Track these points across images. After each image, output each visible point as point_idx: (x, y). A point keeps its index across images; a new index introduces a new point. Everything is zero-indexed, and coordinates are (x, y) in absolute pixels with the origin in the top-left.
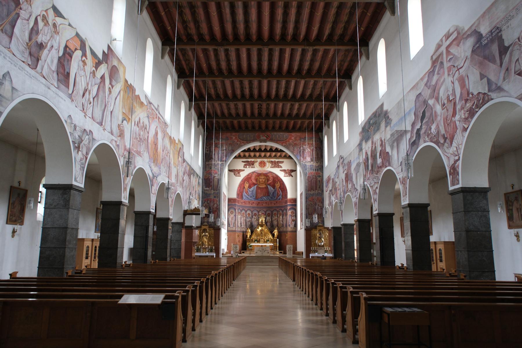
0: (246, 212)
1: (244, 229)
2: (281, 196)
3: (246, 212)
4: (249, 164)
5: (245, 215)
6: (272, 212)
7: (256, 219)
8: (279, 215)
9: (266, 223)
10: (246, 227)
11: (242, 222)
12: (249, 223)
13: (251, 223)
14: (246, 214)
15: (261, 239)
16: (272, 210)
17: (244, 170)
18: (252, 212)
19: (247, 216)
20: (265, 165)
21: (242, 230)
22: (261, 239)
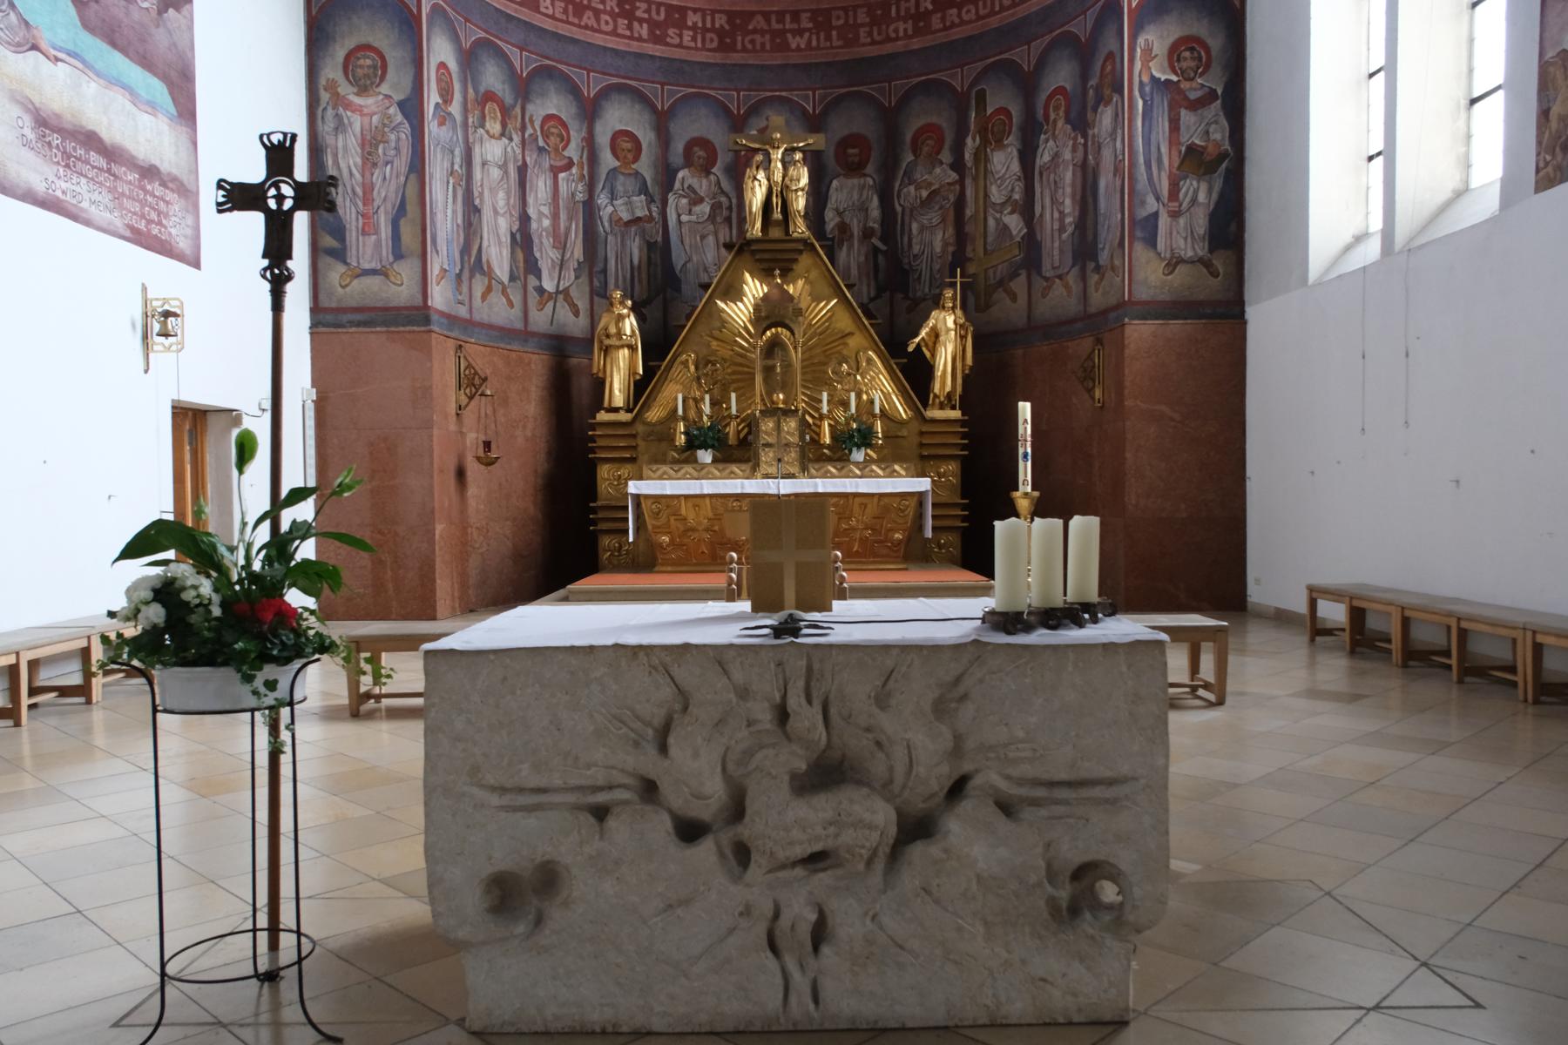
0: (590, 111)
1: (564, 313)
3: (590, 111)
5: (573, 151)
6: (891, 120)
7: (705, 208)
8: (971, 143)
9: (827, 239)
10: (600, 294)
11: (541, 223)
12: (636, 249)
13: (659, 251)
14: (590, 143)
15: (768, 425)
18: (662, 122)
19: (608, 160)
21: (540, 320)
22: (768, 425)
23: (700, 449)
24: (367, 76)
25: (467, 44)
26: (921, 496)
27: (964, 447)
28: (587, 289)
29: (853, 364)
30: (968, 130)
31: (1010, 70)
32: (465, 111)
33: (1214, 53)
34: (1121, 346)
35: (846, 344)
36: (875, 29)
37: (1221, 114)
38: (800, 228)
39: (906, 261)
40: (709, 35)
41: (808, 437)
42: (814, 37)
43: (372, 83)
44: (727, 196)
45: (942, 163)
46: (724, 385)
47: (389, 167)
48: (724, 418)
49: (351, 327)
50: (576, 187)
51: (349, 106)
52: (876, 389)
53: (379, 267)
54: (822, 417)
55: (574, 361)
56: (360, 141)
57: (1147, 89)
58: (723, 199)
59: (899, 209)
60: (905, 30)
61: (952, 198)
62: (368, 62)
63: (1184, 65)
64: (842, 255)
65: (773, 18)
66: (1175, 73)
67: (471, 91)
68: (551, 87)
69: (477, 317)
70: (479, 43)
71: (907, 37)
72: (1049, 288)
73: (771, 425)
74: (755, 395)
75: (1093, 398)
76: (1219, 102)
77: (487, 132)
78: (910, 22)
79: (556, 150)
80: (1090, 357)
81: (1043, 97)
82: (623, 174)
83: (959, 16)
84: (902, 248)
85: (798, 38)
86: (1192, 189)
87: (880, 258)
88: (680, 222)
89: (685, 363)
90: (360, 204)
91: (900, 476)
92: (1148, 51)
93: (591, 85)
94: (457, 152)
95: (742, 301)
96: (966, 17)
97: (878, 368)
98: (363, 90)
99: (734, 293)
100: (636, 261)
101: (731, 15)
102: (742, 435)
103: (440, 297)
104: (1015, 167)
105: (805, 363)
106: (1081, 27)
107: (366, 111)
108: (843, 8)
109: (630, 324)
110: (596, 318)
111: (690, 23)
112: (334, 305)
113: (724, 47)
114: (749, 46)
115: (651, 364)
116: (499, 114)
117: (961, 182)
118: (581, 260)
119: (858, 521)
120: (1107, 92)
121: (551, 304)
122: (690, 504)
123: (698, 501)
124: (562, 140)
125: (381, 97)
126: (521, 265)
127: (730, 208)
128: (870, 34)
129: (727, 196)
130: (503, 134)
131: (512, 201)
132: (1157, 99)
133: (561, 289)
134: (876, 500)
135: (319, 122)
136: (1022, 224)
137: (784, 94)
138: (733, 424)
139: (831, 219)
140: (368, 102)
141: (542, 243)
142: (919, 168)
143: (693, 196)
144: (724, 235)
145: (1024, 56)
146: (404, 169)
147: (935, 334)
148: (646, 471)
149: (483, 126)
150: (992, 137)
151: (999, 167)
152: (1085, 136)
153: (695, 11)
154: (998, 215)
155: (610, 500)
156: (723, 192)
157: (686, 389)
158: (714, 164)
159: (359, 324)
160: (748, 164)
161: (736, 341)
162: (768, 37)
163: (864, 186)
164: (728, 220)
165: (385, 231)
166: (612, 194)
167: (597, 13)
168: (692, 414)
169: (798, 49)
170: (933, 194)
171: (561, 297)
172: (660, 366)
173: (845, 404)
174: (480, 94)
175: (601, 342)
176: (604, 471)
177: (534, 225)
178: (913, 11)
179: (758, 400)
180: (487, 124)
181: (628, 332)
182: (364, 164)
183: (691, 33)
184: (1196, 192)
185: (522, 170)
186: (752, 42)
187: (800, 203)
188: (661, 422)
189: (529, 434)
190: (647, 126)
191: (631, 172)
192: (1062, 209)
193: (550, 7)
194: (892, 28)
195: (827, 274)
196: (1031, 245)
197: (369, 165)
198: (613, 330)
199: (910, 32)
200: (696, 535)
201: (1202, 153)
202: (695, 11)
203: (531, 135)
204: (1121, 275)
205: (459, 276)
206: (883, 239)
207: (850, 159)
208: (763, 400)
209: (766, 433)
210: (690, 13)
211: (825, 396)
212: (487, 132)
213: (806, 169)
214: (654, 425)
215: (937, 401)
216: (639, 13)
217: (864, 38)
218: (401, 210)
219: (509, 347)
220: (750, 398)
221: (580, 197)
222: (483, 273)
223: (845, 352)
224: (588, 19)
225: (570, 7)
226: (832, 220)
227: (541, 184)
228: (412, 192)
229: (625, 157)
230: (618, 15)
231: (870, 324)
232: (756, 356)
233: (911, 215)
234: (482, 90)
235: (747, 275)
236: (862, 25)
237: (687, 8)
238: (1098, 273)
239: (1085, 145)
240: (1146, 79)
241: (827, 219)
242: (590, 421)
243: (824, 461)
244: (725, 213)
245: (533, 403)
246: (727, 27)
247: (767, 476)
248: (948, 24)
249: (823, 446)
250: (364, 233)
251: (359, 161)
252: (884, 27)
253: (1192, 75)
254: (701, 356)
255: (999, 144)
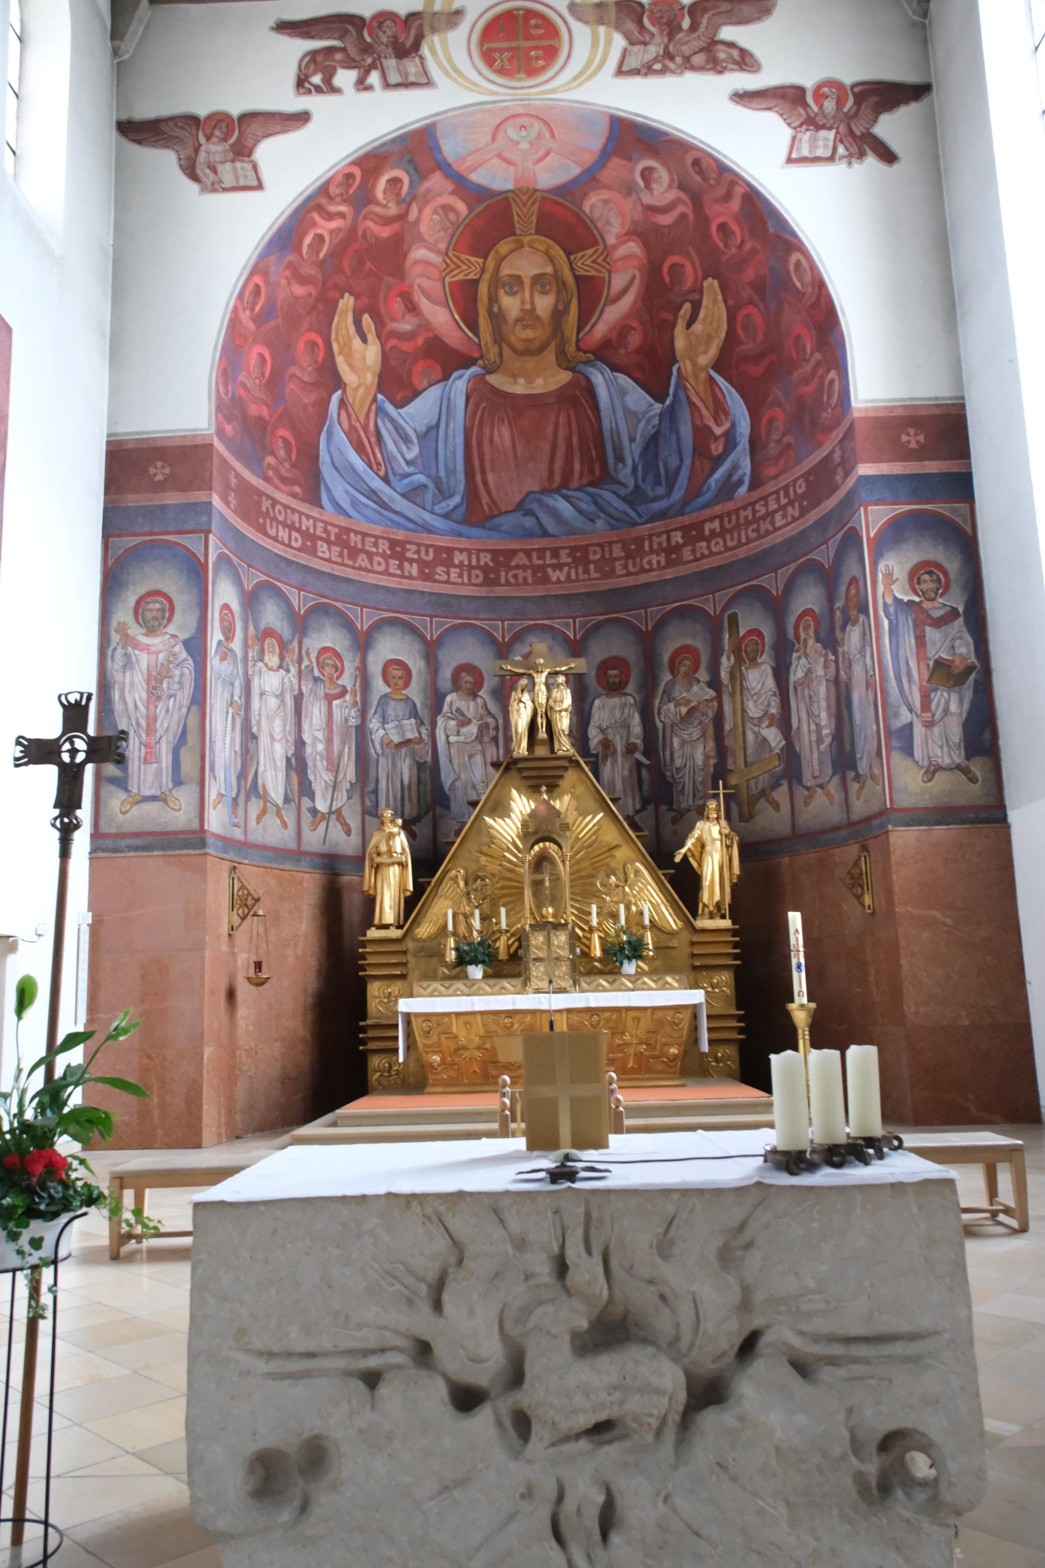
0: (363, 643)
1: (336, 832)
2: (742, 460)
3: (363, 643)
4: (366, 49)
5: (346, 680)
7: (473, 729)
8: (726, 663)
10: (371, 812)
11: (315, 747)
12: (406, 770)
14: (363, 672)
16: (646, 618)
17: (302, 118)
18: (431, 651)
19: (380, 687)
20: (551, 53)
21: (313, 840)
22: (538, 939)
23: (470, 964)
24: (155, 618)
25: (249, 587)
26: (695, 1009)
27: (736, 957)
28: (359, 809)
29: (621, 876)
30: (723, 650)
31: (759, 594)
32: (246, 646)
33: (952, 576)
34: (887, 853)
35: (613, 857)
36: (630, 562)
37: (965, 630)
38: (565, 746)
39: (668, 774)
40: (474, 572)
41: (578, 950)
42: (573, 571)
43: (160, 625)
44: (493, 717)
45: (699, 681)
46: (493, 899)
47: (172, 700)
48: (494, 932)
49: (129, 851)
50: (349, 713)
51: (136, 645)
52: (645, 901)
53: (158, 794)
54: (591, 930)
55: (345, 879)
56: (146, 677)
57: (892, 609)
58: (490, 720)
59: (660, 725)
60: (658, 562)
61: (711, 714)
62: (157, 606)
63: (925, 587)
64: (606, 770)
65: (534, 555)
66: (919, 596)
67: (251, 628)
68: (327, 622)
69: (251, 839)
70: (260, 585)
71: (660, 568)
72: (811, 797)
73: (541, 939)
74: (524, 909)
75: (862, 904)
76: (961, 619)
77: (266, 665)
78: (663, 554)
79: (331, 679)
80: (857, 864)
81: (792, 619)
82: (394, 699)
83: (708, 548)
84: (665, 762)
85: (558, 573)
86: (943, 701)
87: (644, 772)
88: (449, 743)
89: (455, 879)
90: (144, 735)
91: (673, 988)
92: (889, 576)
93: (364, 620)
94: (237, 684)
95: (509, 817)
96: (715, 549)
97: (646, 879)
98: (151, 631)
99: (500, 808)
100: (406, 781)
101: (495, 554)
102: (512, 950)
103: (216, 821)
104: (770, 683)
105: (574, 876)
106: (824, 555)
107: (153, 649)
108: (598, 545)
109: (401, 842)
110: (367, 837)
111: (456, 562)
112: (113, 831)
113: (487, 582)
114: (512, 581)
115: (421, 880)
116: (277, 649)
117: (719, 698)
118: (354, 781)
119: (631, 1036)
120: (853, 613)
121: (323, 824)
122: (461, 1020)
123: (469, 1018)
124: (337, 670)
125: (168, 636)
126: (296, 787)
127: (497, 728)
128: (625, 566)
129: (493, 717)
130: (280, 667)
131: (288, 728)
132: (901, 618)
133: (334, 809)
134: (649, 1011)
135: (109, 661)
136: (780, 737)
137: (546, 622)
138: (503, 938)
139: (594, 737)
140: (156, 642)
141: (315, 766)
142: (677, 687)
143: (461, 718)
144: (491, 753)
145: (772, 582)
146: (186, 702)
147: (702, 845)
148: (416, 988)
149: (262, 660)
150: (745, 656)
151: (754, 685)
152: (835, 653)
153: (461, 551)
154: (756, 729)
155: (381, 1018)
156: (490, 714)
157: (456, 904)
158: (480, 688)
159: (137, 848)
160: (513, 688)
161: (504, 856)
162: (529, 572)
163: (625, 704)
164: (495, 739)
165: (166, 760)
166: (384, 718)
167: (370, 556)
168: (462, 929)
169: (558, 581)
170: (691, 711)
171: (333, 817)
172: (430, 882)
173: (615, 916)
174: (260, 631)
175: (372, 860)
176: (374, 990)
177: (308, 750)
178: (665, 545)
179: (528, 914)
180: (266, 659)
181: (399, 850)
182: (149, 697)
183: (458, 570)
184: (947, 702)
185: (298, 699)
186: (515, 576)
187: (564, 722)
188: (431, 938)
189: (299, 952)
190: (417, 655)
191: (403, 697)
192: (818, 721)
193: (327, 552)
194: (645, 560)
195: (592, 789)
196: (791, 755)
197: (154, 698)
198: (383, 848)
199: (663, 563)
200: (466, 1054)
201: (950, 667)
202: (461, 551)
203: (307, 666)
204: (881, 783)
205: (235, 800)
206: (645, 754)
207: (611, 680)
208: (532, 914)
209: (537, 948)
210: (457, 553)
211: (594, 909)
212: (266, 665)
213: (569, 691)
214: (424, 941)
215: (707, 910)
216: (409, 555)
217: (619, 569)
218: (183, 739)
219: (281, 867)
220: (519, 912)
221: (353, 722)
222: (258, 796)
223: (613, 864)
224: (362, 560)
225: (346, 551)
226: (595, 737)
227: (316, 710)
228: (193, 722)
229: (396, 684)
230: (391, 557)
231: (637, 836)
232: (525, 870)
233: (672, 731)
234: (262, 627)
235: (514, 793)
236: (617, 559)
237: (454, 549)
238: (858, 782)
239: (836, 661)
240: (889, 600)
241: (590, 736)
242: (361, 938)
243: (596, 974)
244: (492, 733)
245: (305, 922)
246: (491, 564)
247: (538, 991)
248: (698, 555)
249: (594, 959)
250: (146, 761)
251: (144, 695)
252: (638, 560)
253: (933, 595)
254: (470, 871)
255: (754, 663)
